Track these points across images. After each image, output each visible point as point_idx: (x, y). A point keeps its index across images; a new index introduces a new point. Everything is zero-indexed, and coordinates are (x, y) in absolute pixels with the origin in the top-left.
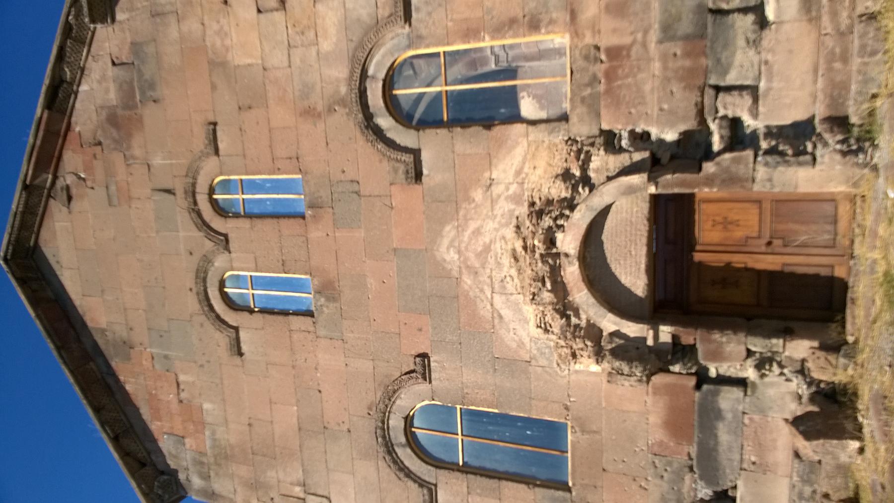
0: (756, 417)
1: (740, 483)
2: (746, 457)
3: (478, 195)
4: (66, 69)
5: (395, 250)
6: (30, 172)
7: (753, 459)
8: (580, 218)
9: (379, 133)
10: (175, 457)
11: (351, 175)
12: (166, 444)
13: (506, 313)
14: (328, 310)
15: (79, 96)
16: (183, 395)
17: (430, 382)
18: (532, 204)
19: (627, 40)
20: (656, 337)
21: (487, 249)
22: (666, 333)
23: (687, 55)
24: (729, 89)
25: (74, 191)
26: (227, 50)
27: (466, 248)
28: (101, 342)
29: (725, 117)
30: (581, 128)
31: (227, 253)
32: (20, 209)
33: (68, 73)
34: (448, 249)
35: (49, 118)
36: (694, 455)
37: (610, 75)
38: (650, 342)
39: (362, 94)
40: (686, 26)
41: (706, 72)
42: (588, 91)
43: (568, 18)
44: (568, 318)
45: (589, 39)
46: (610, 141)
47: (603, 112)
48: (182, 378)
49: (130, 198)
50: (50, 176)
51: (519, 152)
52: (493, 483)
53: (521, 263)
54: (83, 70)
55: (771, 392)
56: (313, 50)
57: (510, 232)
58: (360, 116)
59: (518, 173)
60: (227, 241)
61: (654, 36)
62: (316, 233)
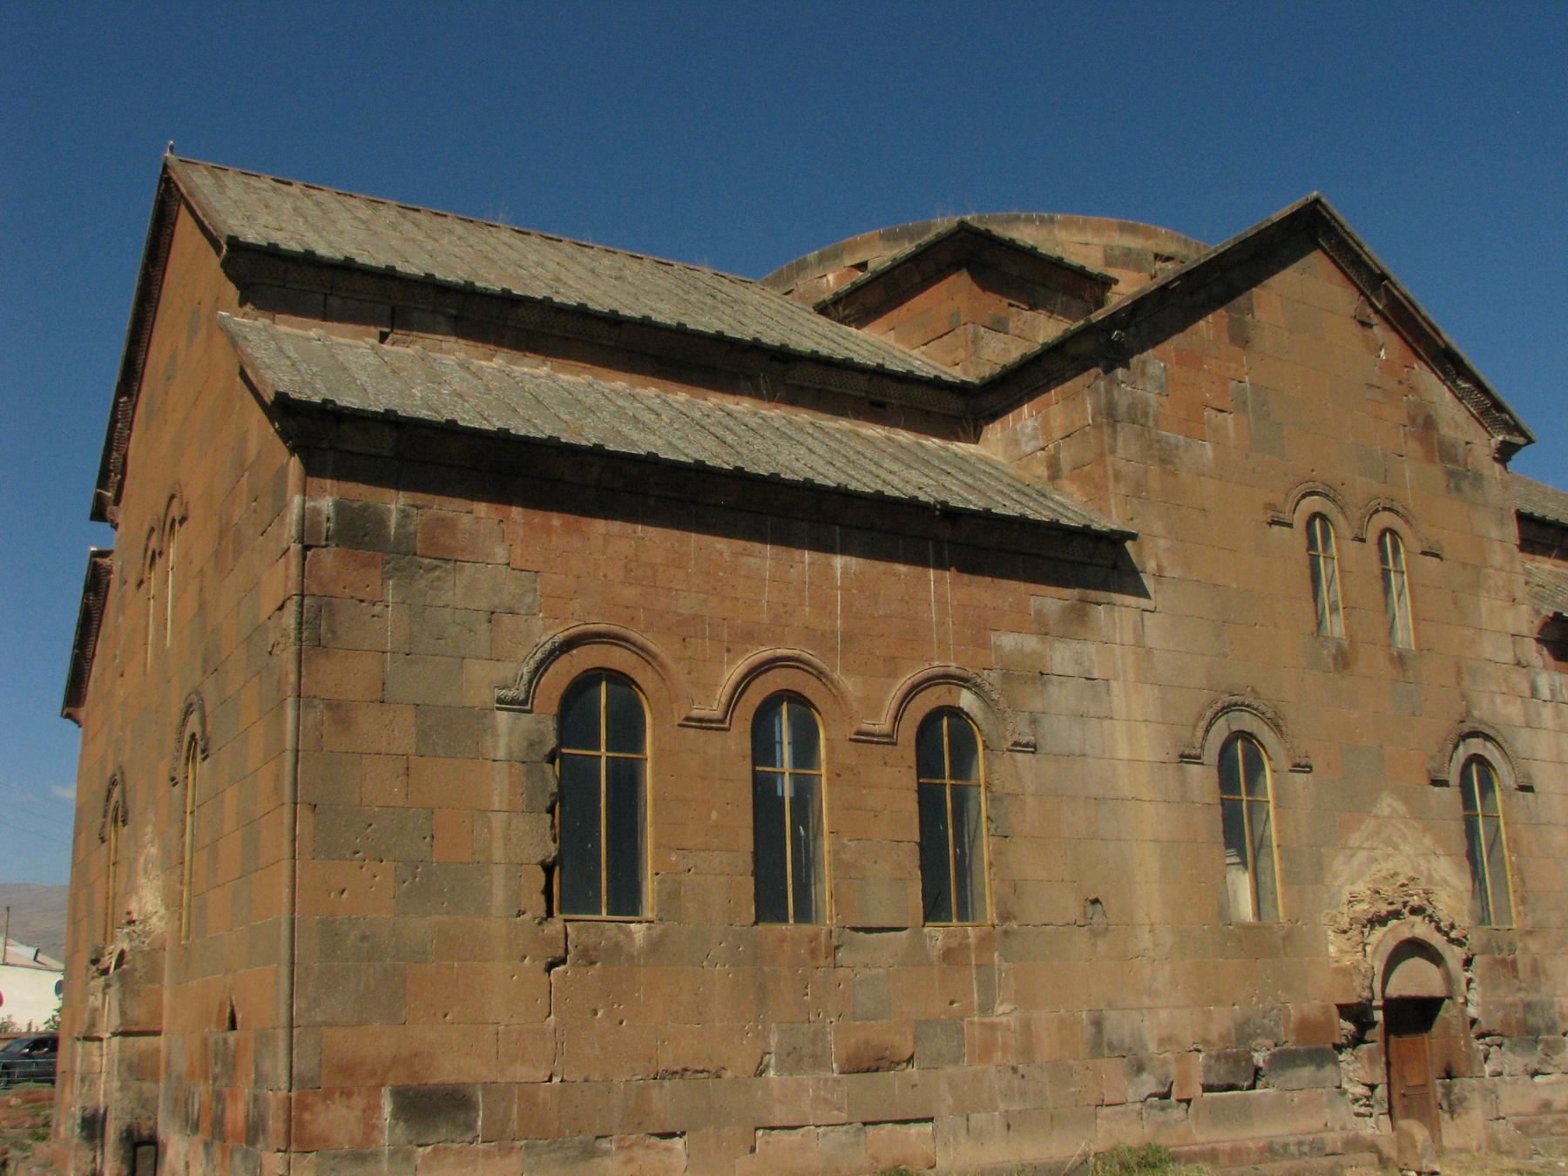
0: (1324, 1099)
1: (1271, 1091)
2: (1295, 1094)
3: (1428, 841)
4: (1467, 385)
5: (1381, 746)
6: (1396, 293)
7: (1296, 1099)
8: (1437, 940)
9: (1456, 747)
10: (1143, 373)
13: (1356, 861)
15: (1440, 383)
17: (1291, 771)
19: (1521, 975)
20: (1377, 1008)
21: (1396, 847)
26: (1488, 592)
27: (1393, 825)
30: (1474, 939)
31: (1352, 536)
32: (1364, 256)
33: (1464, 385)
34: (1390, 806)
35: (1436, 342)
36: (1285, 1047)
37: (1504, 960)
40: (1531, 1020)
41: (1509, 1037)
42: (1494, 944)
43: (1528, 928)
45: (1519, 945)
47: (1485, 957)
50: (1381, 307)
51: (1454, 881)
53: (1391, 881)
54: (1460, 399)
55: (1343, 1109)
59: (1445, 881)
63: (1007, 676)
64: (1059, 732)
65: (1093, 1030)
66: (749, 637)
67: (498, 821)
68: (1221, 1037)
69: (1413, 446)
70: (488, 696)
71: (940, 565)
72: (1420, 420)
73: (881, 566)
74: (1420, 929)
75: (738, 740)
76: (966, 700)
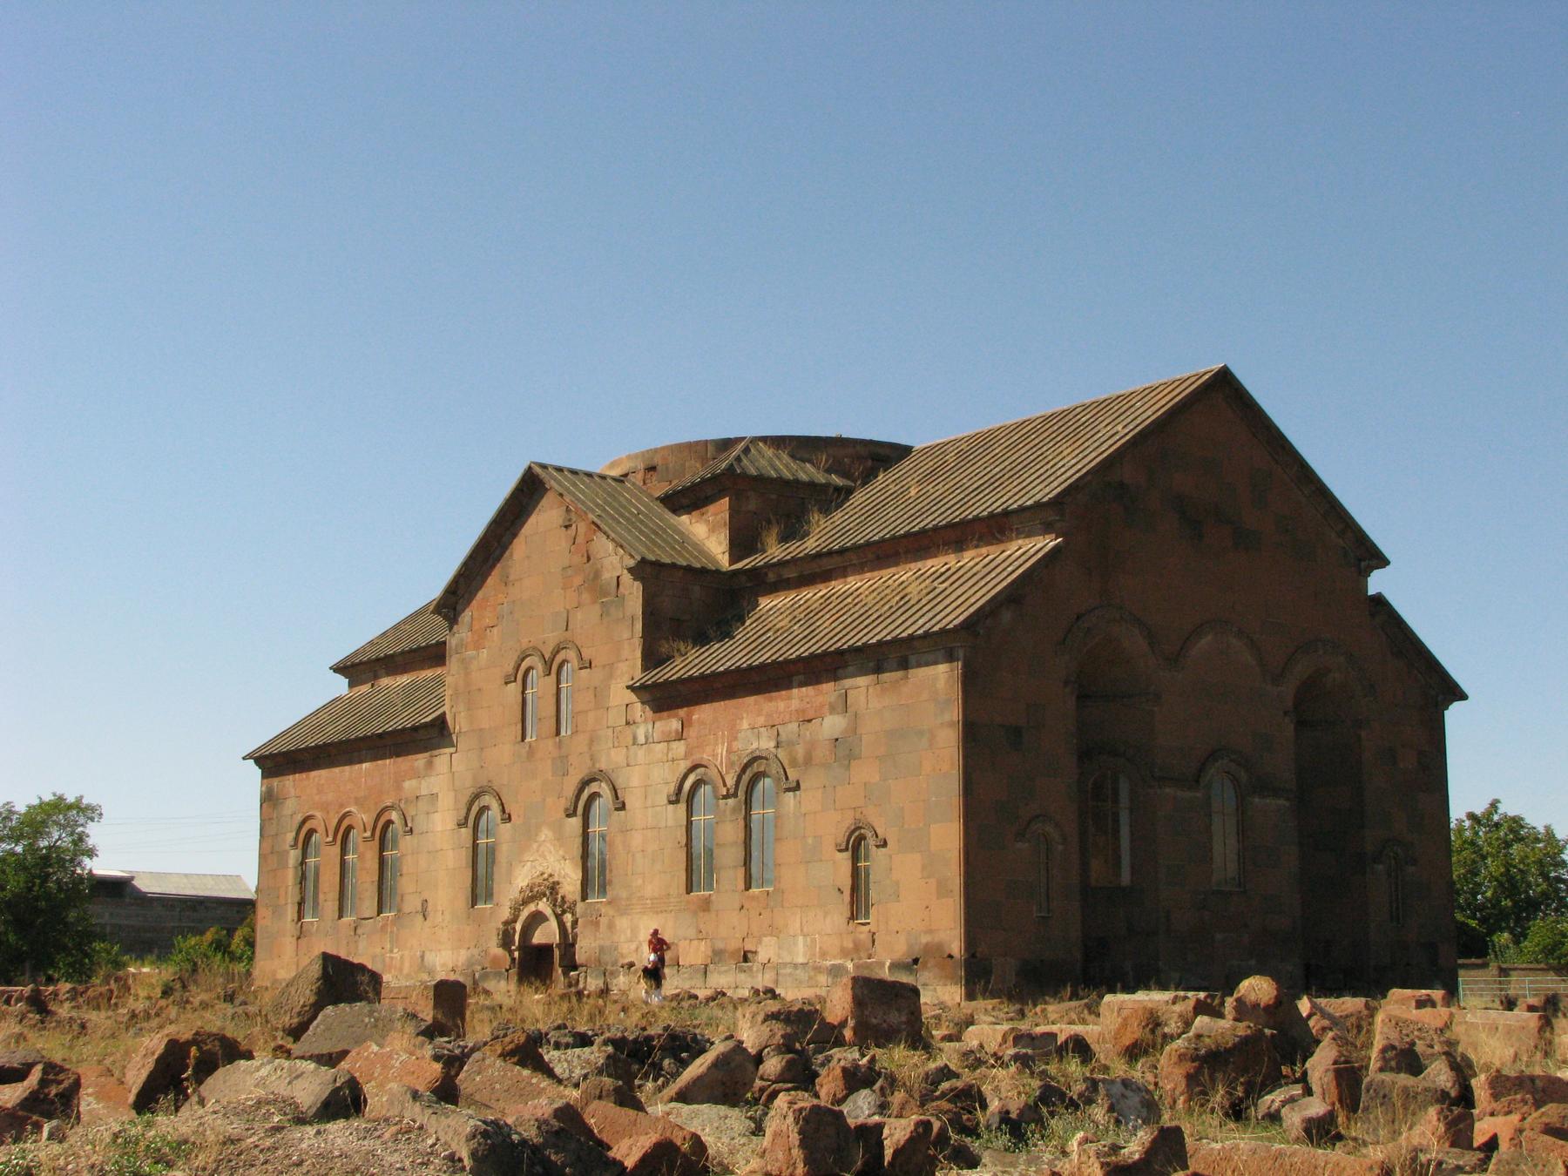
5: (544, 800)
8: (548, 911)
9: (581, 791)
11: (571, 770)
12: (466, 617)
14: (524, 749)
16: (488, 631)
18: (558, 883)
19: (601, 930)
22: (516, 954)
23: (595, 959)
24: (586, 977)
25: (569, 532)
28: (507, 553)
29: (579, 975)
37: (592, 921)
38: (513, 948)
39: (593, 780)
44: (523, 905)
46: (575, 923)
48: (495, 630)
49: (564, 589)
52: (471, 864)
56: (611, 745)
57: (550, 871)
58: (586, 779)
60: (548, 675)
61: (602, 942)
62: (550, 744)
63: (407, 801)
64: (420, 824)
65: (420, 960)
66: (342, 806)
67: (290, 888)
68: (463, 965)
69: (586, 597)
70: (288, 847)
71: (390, 757)
72: (592, 575)
73: (374, 763)
74: (544, 906)
75: (337, 849)
76: (394, 816)
